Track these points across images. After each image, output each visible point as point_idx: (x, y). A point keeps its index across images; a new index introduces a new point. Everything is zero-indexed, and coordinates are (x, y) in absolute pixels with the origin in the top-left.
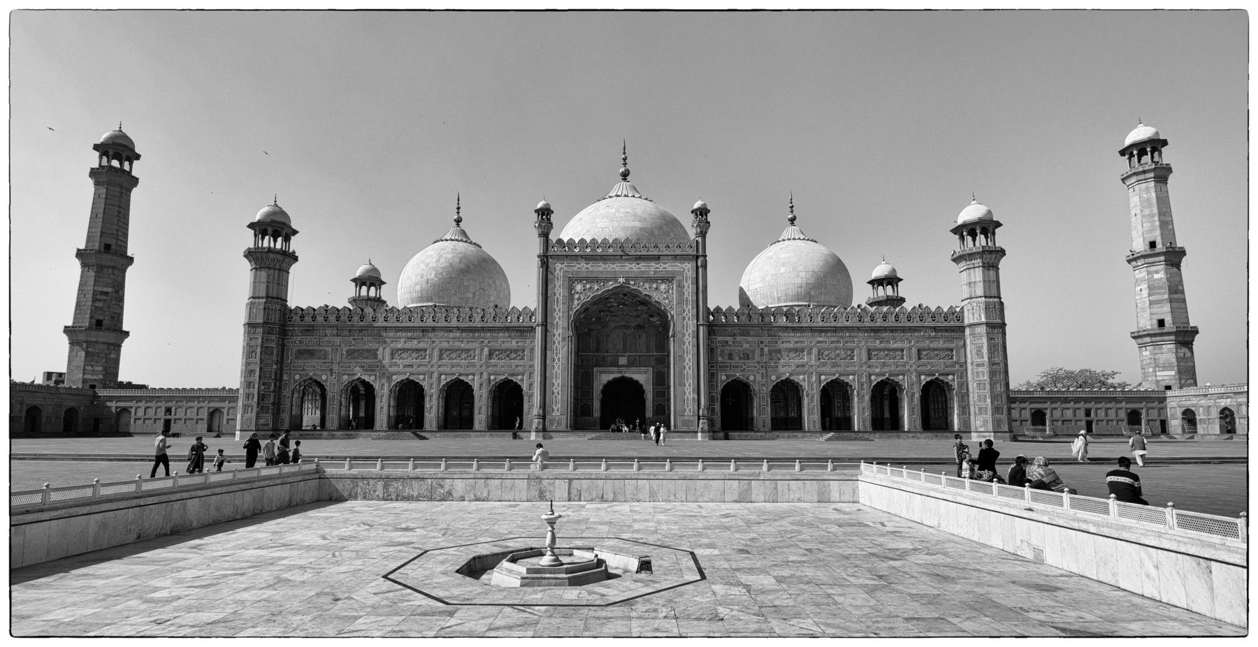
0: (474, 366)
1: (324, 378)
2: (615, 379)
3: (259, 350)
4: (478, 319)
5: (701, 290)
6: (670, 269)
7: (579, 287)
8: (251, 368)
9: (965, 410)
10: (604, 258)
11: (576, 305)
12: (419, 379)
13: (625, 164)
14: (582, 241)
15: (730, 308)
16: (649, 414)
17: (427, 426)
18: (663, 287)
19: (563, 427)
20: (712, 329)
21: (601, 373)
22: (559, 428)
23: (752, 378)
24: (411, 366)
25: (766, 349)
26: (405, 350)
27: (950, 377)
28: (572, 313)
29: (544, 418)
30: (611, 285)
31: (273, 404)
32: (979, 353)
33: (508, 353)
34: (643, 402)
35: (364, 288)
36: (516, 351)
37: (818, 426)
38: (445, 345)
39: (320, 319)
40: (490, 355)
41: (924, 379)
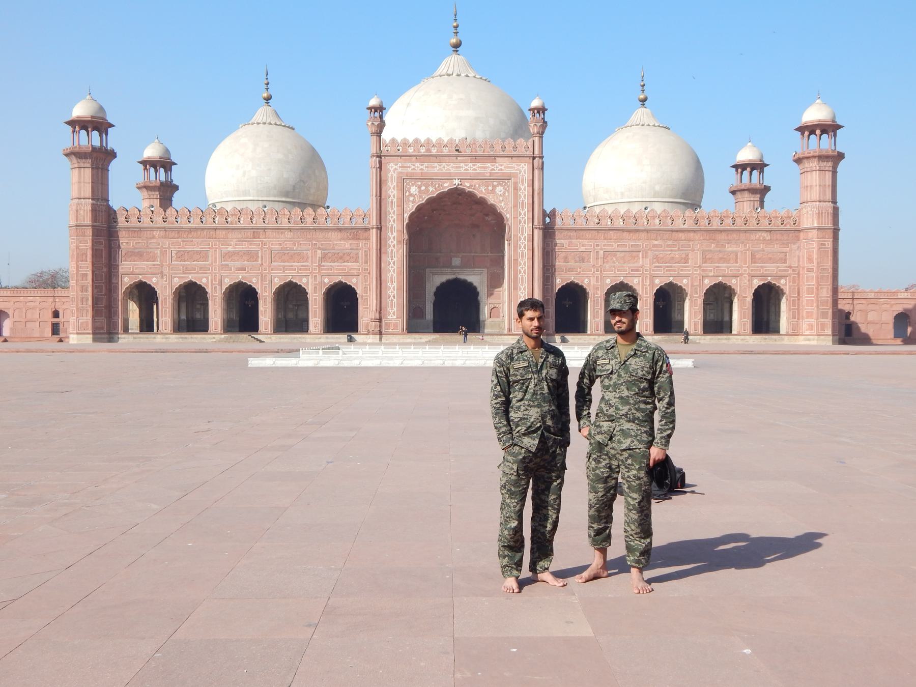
0: (306, 268)
2: (449, 282)
3: (89, 253)
4: (309, 220)
5: (537, 193)
7: (414, 190)
8: (82, 271)
9: (796, 315)
10: (439, 157)
11: (411, 208)
12: (254, 282)
14: (417, 141)
18: (499, 190)
19: (399, 330)
20: (548, 232)
21: (434, 274)
22: (395, 331)
23: (586, 281)
24: (243, 269)
26: (234, 253)
27: (783, 281)
28: (406, 216)
29: (380, 320)
30: (447, 186)
31: (106, 307)
32: (810, 260)
33: (341, 257)
36: (349, 255)
38: (277, 248)
39: (146, 221)
40: (324, 257)
41: (757, 283)
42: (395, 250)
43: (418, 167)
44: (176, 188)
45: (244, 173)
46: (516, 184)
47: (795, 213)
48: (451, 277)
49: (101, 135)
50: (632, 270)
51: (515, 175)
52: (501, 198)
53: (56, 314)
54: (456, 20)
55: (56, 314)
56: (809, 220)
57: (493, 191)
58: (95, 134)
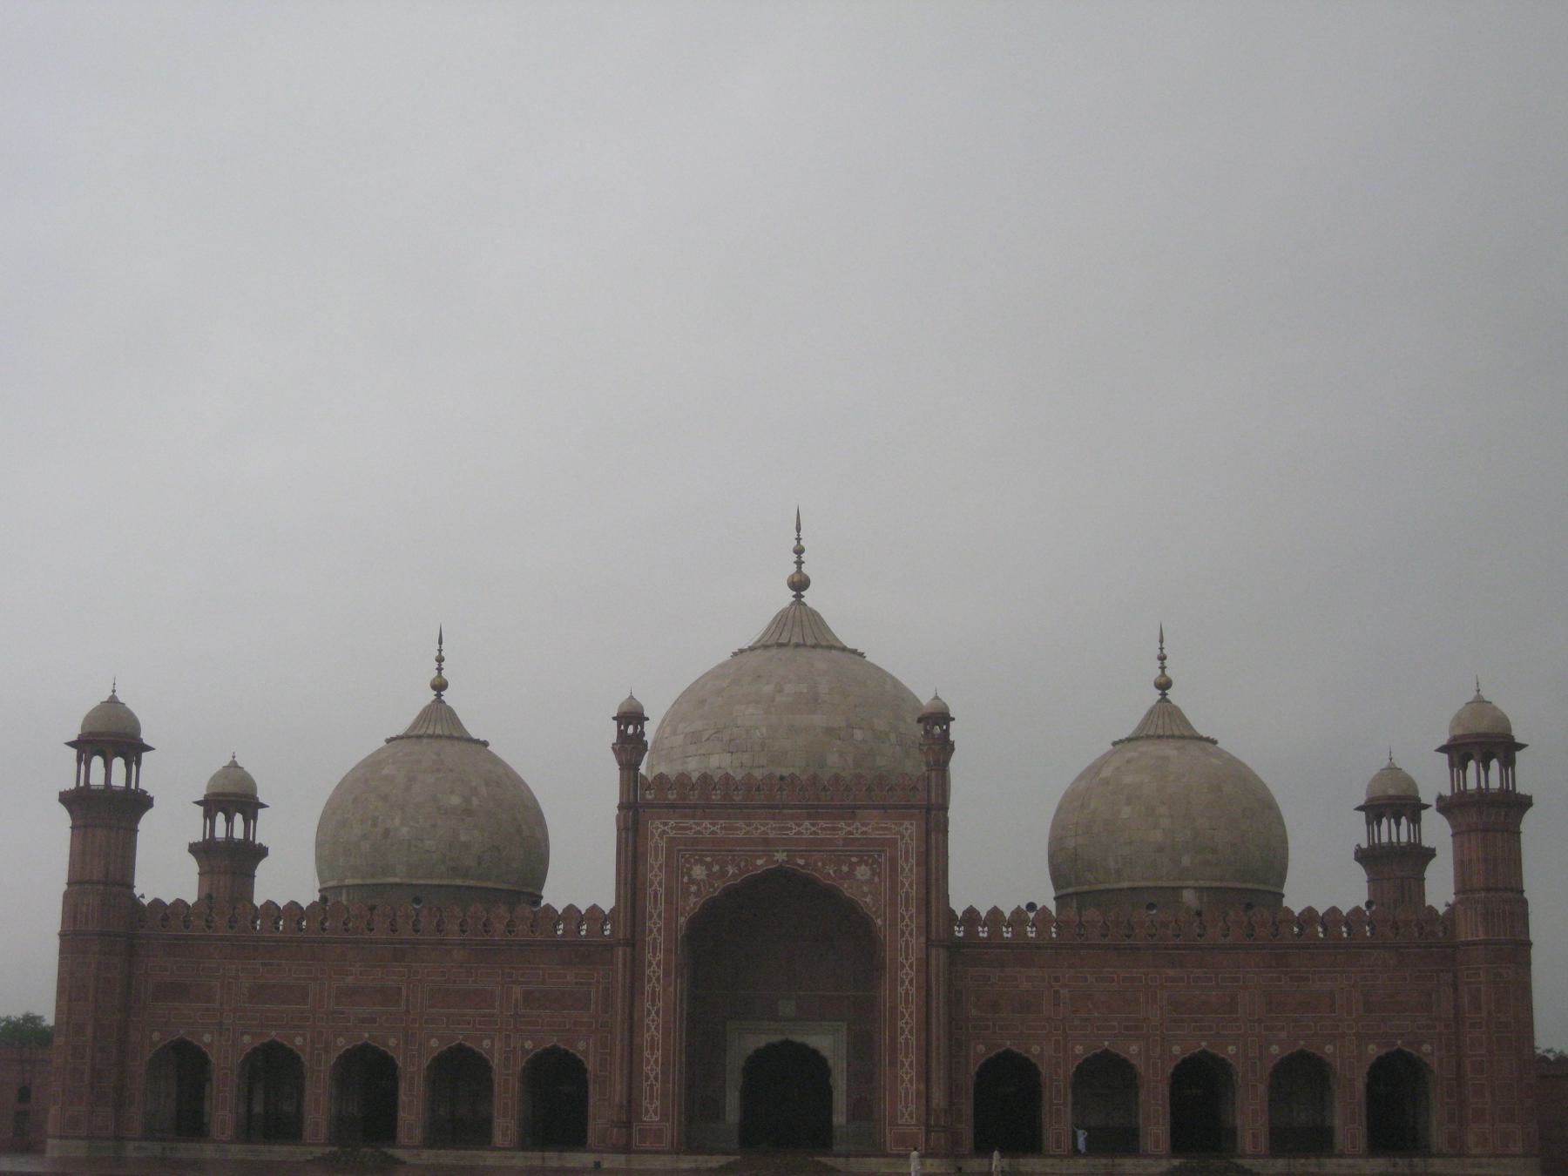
1: (207, 1038)
2: (771, 1048)
6: (875, 835)
7: (699, 872)
11: (693, 903)
13: (799, 563)
14: (705, 778)
15: (995, 912)
16: (839, 1119)
17: (402, 1135)
18: (862, 872)
23: (1035, 1049)
24: (373, 1020)
25: (1064, 992)
27: (1426, 1048)
28: (682, 920)
29: (628, 1125)
34: (826, 1093)
35: (220, 818)
37: (1165, 1145)
41: (1373, 1051)
42: (659, 989)
43: (708, 827)
44: (261, 852)
45: (387, 831)
46: (893, 862)
47: (1442, 910)
48: (776, 1038)
49: (128, 766)
50: (1127, 1028)
51: (892, 843)
52: (865, 889)
53: (24, 1094)
54: (799, 539)
55: (24, 1094)
56: (1470, 930)
57: (850, 875)
58: (118, 764)
